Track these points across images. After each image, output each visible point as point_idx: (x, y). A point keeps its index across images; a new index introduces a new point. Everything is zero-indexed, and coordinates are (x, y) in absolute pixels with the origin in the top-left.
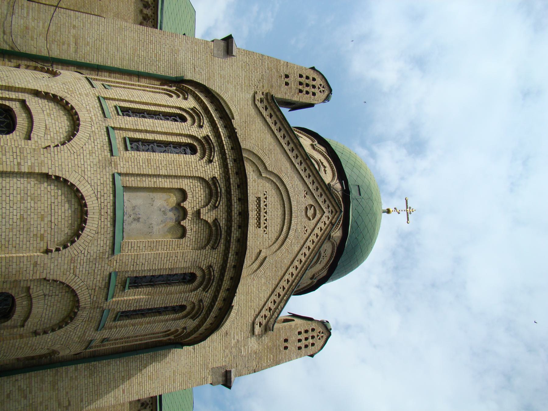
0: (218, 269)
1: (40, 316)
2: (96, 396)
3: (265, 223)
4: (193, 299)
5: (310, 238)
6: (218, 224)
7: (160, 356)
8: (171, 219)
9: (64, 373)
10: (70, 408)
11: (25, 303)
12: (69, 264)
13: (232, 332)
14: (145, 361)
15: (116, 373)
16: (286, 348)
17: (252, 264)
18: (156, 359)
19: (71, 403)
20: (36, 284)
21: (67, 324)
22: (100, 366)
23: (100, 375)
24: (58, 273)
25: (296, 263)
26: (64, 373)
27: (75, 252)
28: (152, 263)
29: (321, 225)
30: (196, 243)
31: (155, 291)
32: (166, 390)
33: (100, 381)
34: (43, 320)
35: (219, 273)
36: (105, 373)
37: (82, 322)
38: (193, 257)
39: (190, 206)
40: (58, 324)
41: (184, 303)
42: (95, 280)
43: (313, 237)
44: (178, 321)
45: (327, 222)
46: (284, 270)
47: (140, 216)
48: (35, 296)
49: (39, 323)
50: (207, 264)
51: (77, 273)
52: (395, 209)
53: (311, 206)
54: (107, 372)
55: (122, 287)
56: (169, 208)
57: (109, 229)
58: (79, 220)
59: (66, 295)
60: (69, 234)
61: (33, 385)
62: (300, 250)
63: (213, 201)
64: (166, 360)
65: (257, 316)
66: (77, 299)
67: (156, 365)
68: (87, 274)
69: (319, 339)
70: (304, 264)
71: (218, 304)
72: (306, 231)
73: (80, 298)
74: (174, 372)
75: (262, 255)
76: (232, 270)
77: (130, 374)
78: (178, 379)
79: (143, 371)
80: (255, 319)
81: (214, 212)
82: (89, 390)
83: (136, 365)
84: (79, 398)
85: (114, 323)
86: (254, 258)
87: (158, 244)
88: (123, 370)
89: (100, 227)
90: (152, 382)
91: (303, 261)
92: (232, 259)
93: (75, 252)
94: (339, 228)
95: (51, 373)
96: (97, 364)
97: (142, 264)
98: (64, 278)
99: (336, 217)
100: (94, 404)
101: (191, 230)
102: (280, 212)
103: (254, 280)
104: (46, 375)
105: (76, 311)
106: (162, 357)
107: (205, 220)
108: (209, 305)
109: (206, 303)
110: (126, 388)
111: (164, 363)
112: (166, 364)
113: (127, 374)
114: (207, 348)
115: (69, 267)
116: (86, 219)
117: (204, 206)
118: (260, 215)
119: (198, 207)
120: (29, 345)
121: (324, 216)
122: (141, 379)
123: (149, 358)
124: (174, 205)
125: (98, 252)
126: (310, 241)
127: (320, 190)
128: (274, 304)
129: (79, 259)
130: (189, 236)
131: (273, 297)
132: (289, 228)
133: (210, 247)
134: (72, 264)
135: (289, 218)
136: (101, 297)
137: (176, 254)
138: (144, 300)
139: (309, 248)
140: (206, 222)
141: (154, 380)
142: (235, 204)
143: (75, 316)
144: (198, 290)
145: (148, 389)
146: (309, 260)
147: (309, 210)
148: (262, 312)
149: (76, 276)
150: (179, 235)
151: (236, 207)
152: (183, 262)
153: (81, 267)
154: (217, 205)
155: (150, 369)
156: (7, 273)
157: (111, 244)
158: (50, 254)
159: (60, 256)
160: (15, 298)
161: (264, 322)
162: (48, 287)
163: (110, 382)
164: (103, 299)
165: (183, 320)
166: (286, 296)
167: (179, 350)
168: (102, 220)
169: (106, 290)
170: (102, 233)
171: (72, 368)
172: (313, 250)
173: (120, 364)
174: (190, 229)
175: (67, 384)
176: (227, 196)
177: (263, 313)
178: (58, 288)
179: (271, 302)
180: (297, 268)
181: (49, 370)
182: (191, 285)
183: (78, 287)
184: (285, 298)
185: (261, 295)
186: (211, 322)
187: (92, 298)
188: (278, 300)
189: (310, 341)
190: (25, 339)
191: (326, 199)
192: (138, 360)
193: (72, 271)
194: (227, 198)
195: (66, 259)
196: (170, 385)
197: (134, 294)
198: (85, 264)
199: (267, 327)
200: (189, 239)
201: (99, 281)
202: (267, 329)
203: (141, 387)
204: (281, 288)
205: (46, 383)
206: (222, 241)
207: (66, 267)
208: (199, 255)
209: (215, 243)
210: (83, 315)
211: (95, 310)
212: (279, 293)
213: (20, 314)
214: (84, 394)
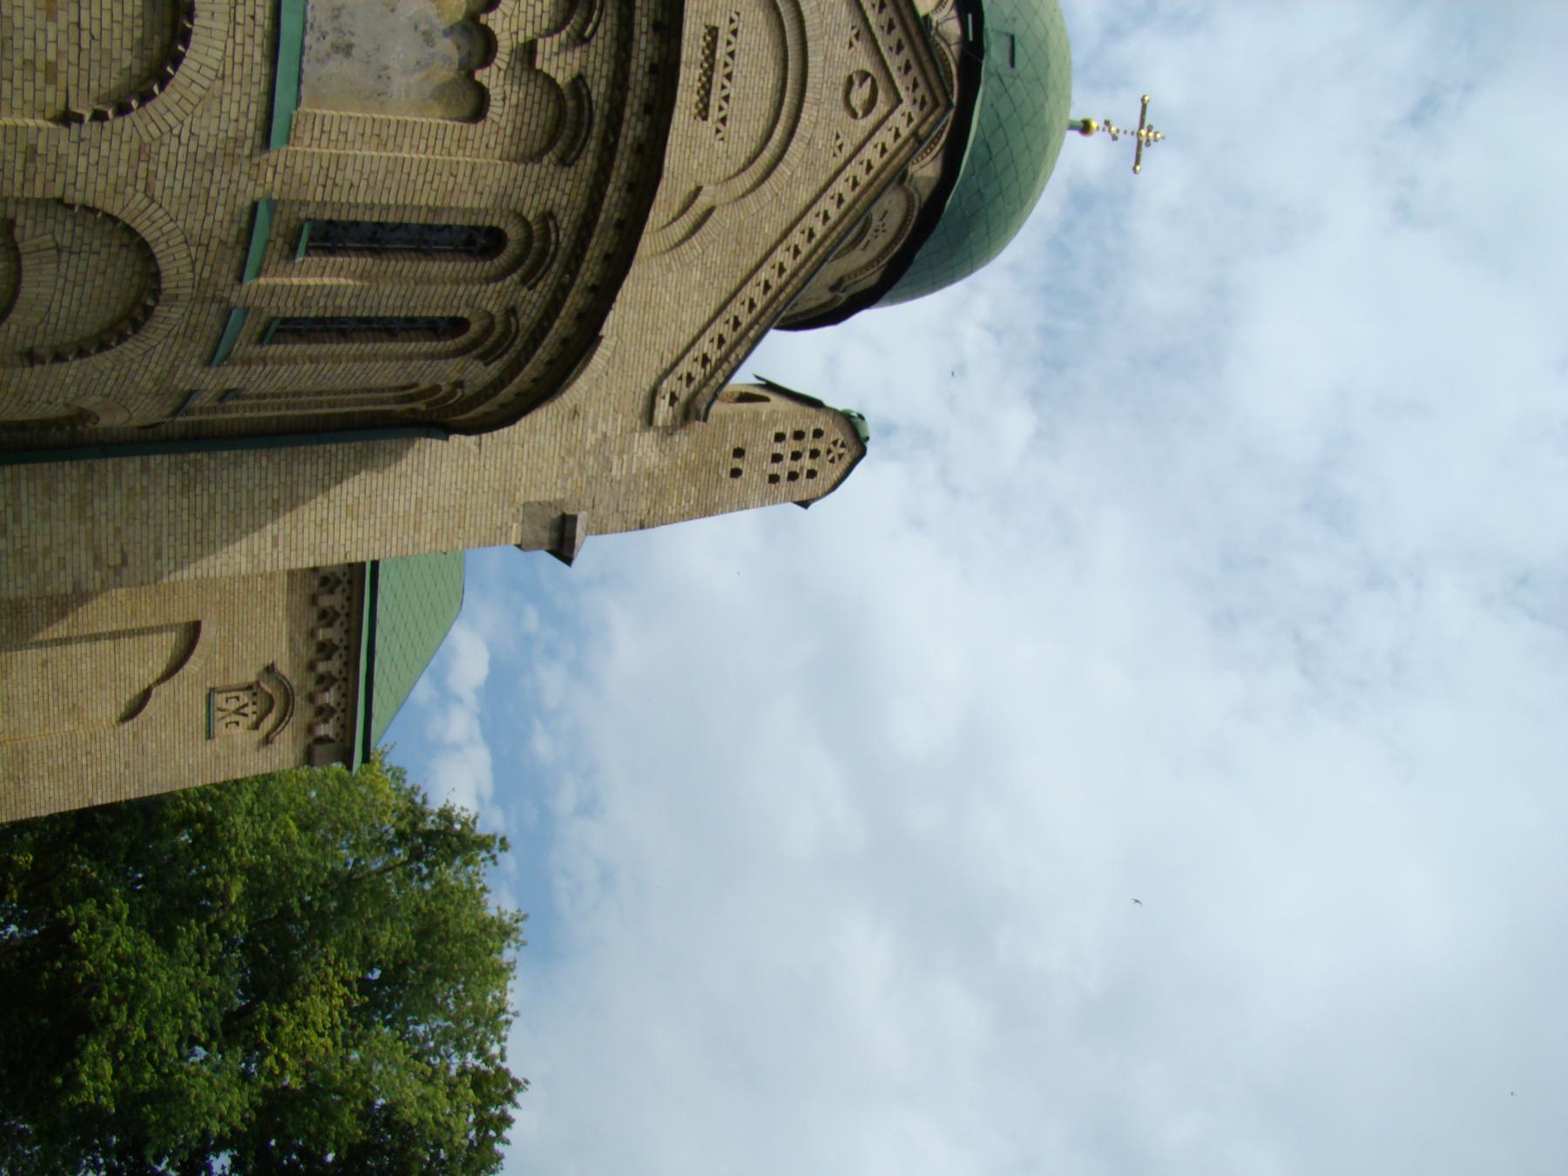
0: (570, 227)
1: (44, 310)
3: (721, 109)
4: (491, 303)
5: (849, 171)
6: (584, 92)
7: (382, 454)
8: (446, 58)
9: (110, 475)
10: (125, 571)
14: (340, 464)
16: (736, 473)
17: (670, 223)
18: (370, 462)
19: (130, 559)
20: (32, 212)
21: (122, 338)
22: (212, 466)
23: (212, 490)
24: (100, 187)
25: (797, 238)
26: (110, 475)
27: (152, 128)
28: (379, 185)
29: (885, 136)
30: (515, 140)
31: (383, 268)
33: (212, 508)
34: (53, 320)
35: (573, 238)
37: (168, 336)
38: (503, 183)
39: (506, 26)
41: (464, 313)
42: (209, 219)
43: (856, 170)
44: (442, 363)
45: (905, 132)
46: (760, 253)
47: (353, 40)
48: (29, 249)
49: (41, 328)
50: (541, 208)
51: (158, 193)
52: (1107, 123)
53: (865, 75)
54: (231, 484)
55: (286, 247)
56: (442, 24)
57: (257, 70)
58: (167, 32)
60: (136, 71)
61: (24, 499)
62: (814, 202)
63: (576, 19)
64: (398, 468)
65: (667, 373)
66: (153, 270)
69: (832, 461)
71: (561, 326)
72: (840, 147)
74: (419, 501)
75: (703, 201)
76: (611, 233)
77: (294, 497)
78: (429, 523)
79: (332, 491)
81: (577, 54)
82: (179, 530)
83: (314, 473)
85: (258, 349)
87: (401, 130)
88: (276, 483)
89: (229, 61)
91: (818, 235)
92: (615, 199)
93: (152, 128)
94: (934, 153)
95: (75, 472)
96: (206, 460)
97: (352, 186)
98: (119, 204)
99: (931, 119)
100: (193, 566)
101: (504, 99)
102: (770, 82)
103: (669, 269)
104: (60, 478)
105: (150, 303)
106: (388, 457)
107: (547, 77)
108: (533, 326)
109: (526, 320)
110: (281, 533)
111: (392, 475)
114: (517, 447)
116: (189, 32)
117: (549, 33)
118: (710, 80)
119: (529, 34)
120: (12, 389)
121: (897, 113)
122: (325, 512)
124: (460, 17)
125: (222, 135)
126: (847, 180)
127: (898, 32)
128: (719, 347)
129: (164, 151)
130: (497, 118)
131: (720, 327)
132: (790, 134)
133: (554, 158)
134: (143, 165)
135: (795, 102)
136: (224, 271)
137: (454, 165)
138: (349, 291)
139: (841, 200)
140: (550, 81)
141: (361, 519)
142: (644, 38)
143: (146, 319)
144: (508, 281)
145: (342, 542)
146: (834, 235)
147: (857, 83)
148: (681, 364)
149: (152, 200)
150: (467, 111)
151: (643, 45)
152: (470, 195)
154: (587, 33)
155: (354, 488)
157: (261, 116)
158: (75, 126)
159: (106, 134)
161: (684, 393)
162: (69, 226)
163: (237, 512)
164: (231, 276)
165: (458, 359)
166: (756, 327)
167: (436, 444)
168: (239, 40)
169: (239, 253)
170: (237, 78)
171: (133, 464)
172: (850, 207)
173: (270, 465)
174: (499, 97)
175: (118, 505)
176: (620, 9)
177: (685, 367)
179: (712, 341)
180: (797, 252)
181: (67, 463)
182: (488, 263)
183: (158, 234)
184: (752, 334)
185: (686, 317)
186: (535, 375)
187: (198, 269)
188: (730, 337)
189: (806, 462)
191: (912, 63)
192: (321, 461)
193: (141, 186)
194: (620, 16)
195: (125, 147)
197: (319, 272)
198: (181, 168)
199: (692, 409)
200: (495, 128)
201: (220, 221)
202: (690, 413)
203: (325, 534)
204: (743, 303)
205: (61, 500)
206: (592, 144)
207: (123, 170)
208: (520, 178)
209: (570, 147)
210: (170, 316)
212: (736, 318)
214: (164, 539)
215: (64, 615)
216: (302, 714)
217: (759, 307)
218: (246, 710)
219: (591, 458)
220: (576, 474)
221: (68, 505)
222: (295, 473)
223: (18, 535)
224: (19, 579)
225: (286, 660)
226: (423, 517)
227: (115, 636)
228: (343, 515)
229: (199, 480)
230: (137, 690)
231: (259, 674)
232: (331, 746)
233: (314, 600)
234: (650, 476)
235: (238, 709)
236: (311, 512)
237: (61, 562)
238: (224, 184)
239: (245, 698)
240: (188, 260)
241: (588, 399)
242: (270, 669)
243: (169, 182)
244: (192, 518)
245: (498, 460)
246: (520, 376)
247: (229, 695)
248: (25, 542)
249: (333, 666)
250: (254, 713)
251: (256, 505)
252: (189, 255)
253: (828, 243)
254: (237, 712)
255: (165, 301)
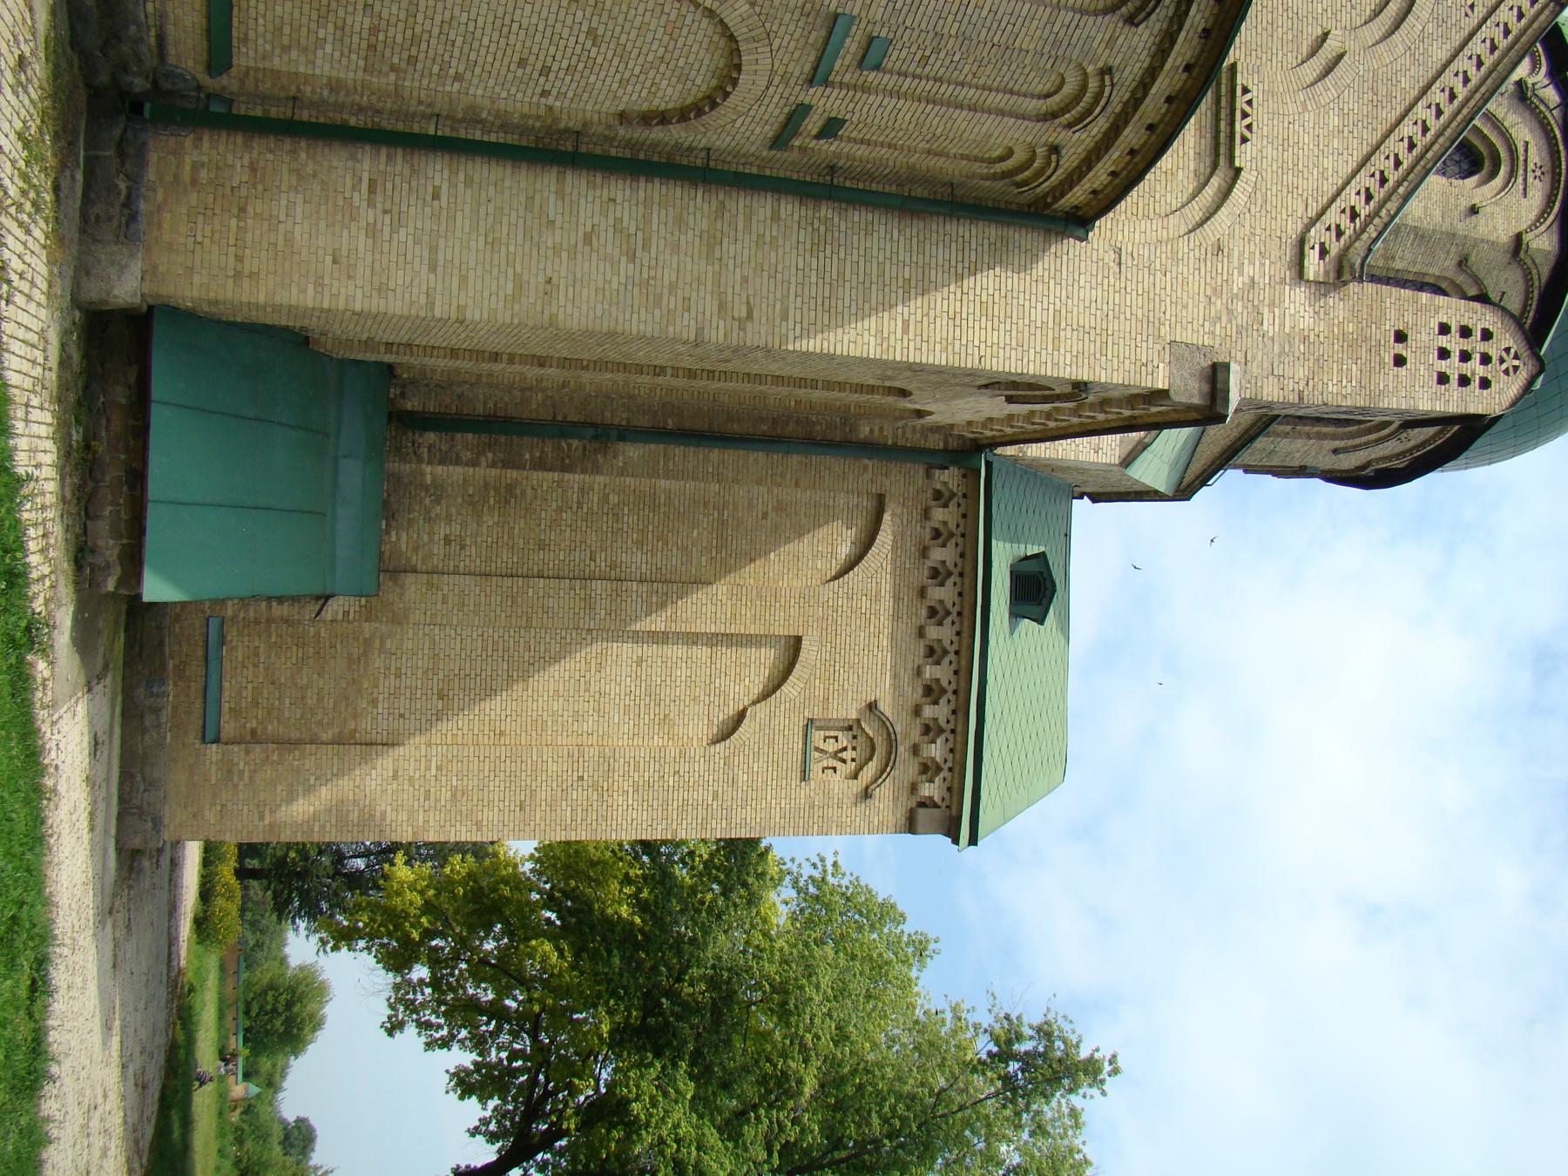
2: (826, 315)
7: (1016, 251)
9: (741, 217)
10: (749, 325)
13: (1236, 249)
14: (973, 253)
15: (888, 262)
16: (1400, 361)
18: (1004, 257)
22: (843, 228)
23: (842, 255)
26: (741, 217)
32: (1031, 364)
33: (841, 274)
36: (855, 251)
44: (1092, 19)
46: (1399, 110)
54: (862, 253)
61: (655, 227)
64: (1034, 271)
65: (1313, 222)
67: (1003, 274)
69: (1506, 372)
70: (1463, 105)
77: (926, 279)
78: (1069, 342)
79: (965, 282)
80: (1307, 229)
82: (806, 289)
83: (947, 257)
84: (778, 305)
86: (1305, 51)
88: (908, 260)
90: (989, 324)
91: (1460, 97)
95: (706, 206)
96: (836, 220)
100: (819, 336)
103: (1305, 109)
104: (691, 210)
106: (1023, 255)
110: (913, 317)
112: (1034, 284)
113: (920, 278)
122: (958, 303)
123: (986, 247)
126: (1484, 41)
131: (1364, 180)
141: (996, 319)
145: (977, 343)
146: (1478, 96)
148: (1328, 212)
155: (988, 282)
161: (1335, 248)
163: (867, 285)
166: (1406, 184)
167: (1072, 246)
171: (763, 206)
173: (902, 238)
175: (746, 252)
177: (1332, 217)
179: (1358, 193)
180: (1439, 113)
184: (1401, 190)
185: (1328, 163)
188: (1379, 194)
189: (1475, 368)
196: (1044, 352)
199: (1345, 263)
203: (958, 329)
204: (1387, 158)
205: (690, 233)
212: (1382, 172)
214: (792, 298)
215: (662, 606)
216: (906, 769)
217: (1405, 165)
218: (844, 755)
219: (1240, 304)
220: (1224, 319)
221: (697, 240)
222: (927, 254)
223: (646, 263)
224: (643, 311)
225: (889, 699)
226: (1062, 333)
227: (715, 640)
228: (978, 311)
229: (829, 241)
230: (731, 711)
231: (860, 711)
232: (936, 811)
233: (921, 632)
234: (1305, 339)
235: (836, 753)
236: (944, 301)
237: (686, 302)
239: (844, 740)
241: (1231, 236)
242: (872, 707)
244: (820, 281)
245: (1140, 285)
246: (1173, 55)
247: (827, 734)
248: (652, 273)
249: (939, 712)
250: (853, 760)
251: (887, 282)
253: (1472, 103)
254: (835, 755)
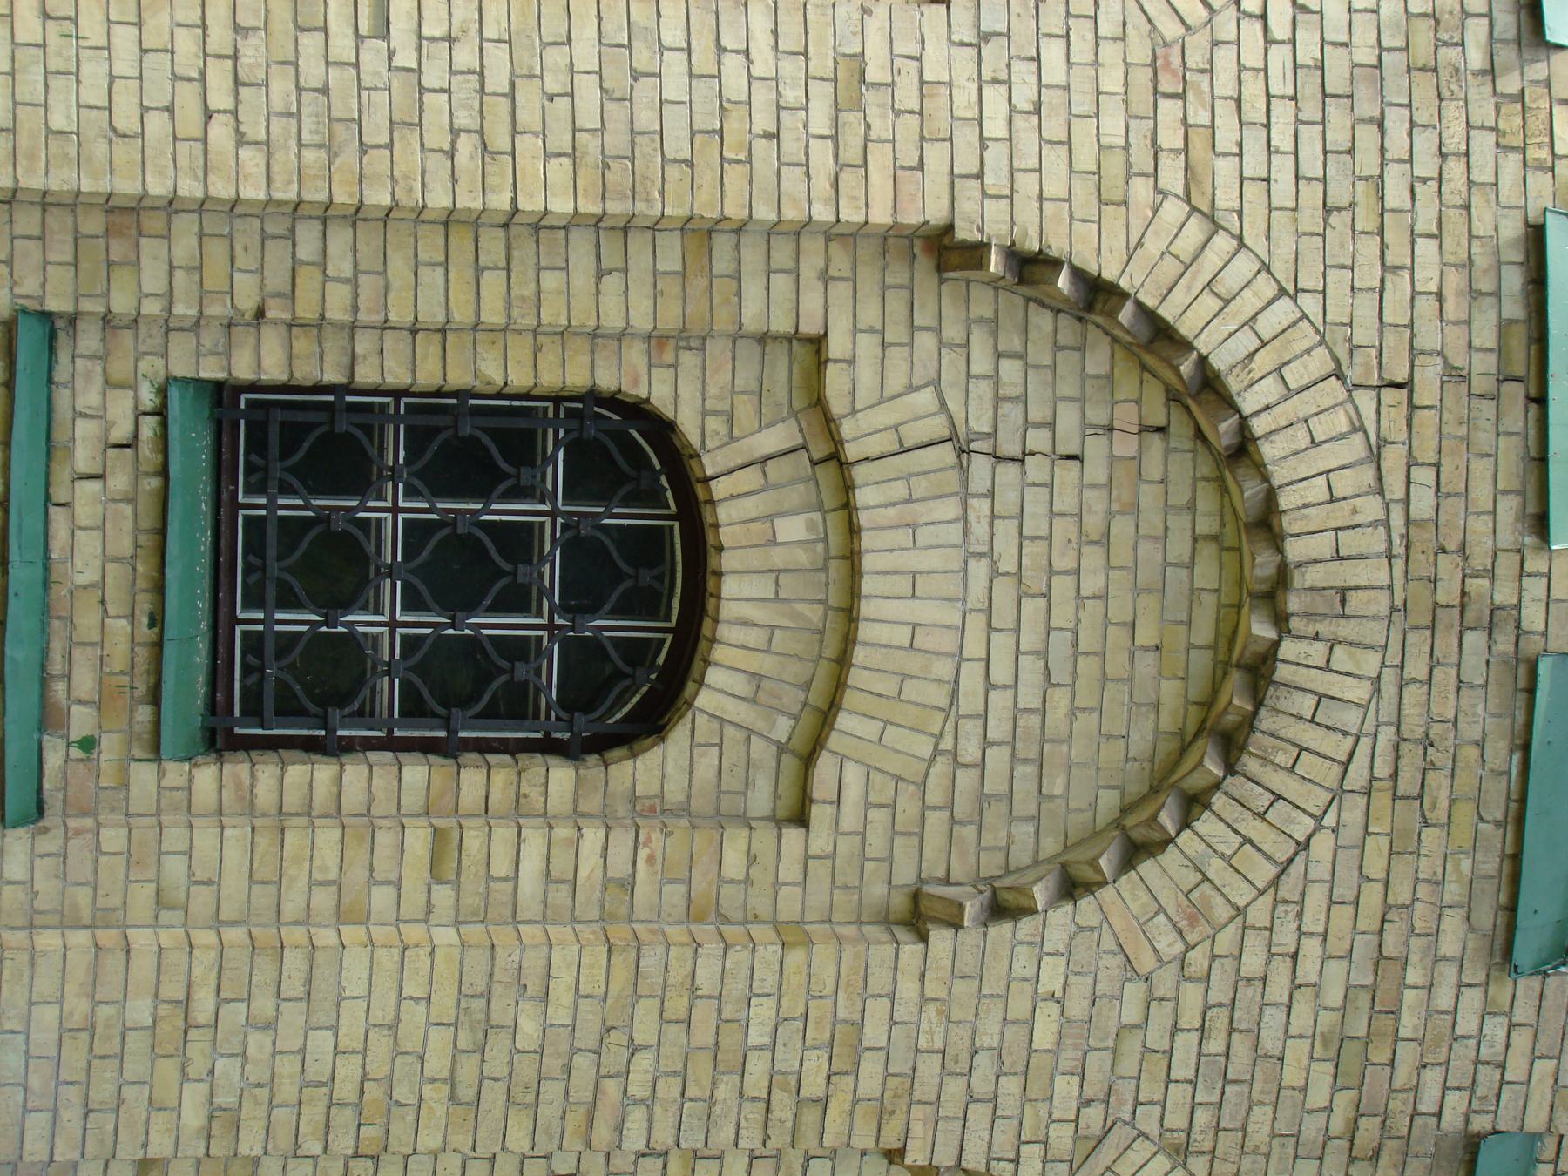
1: (941, 697)
11: (793, 529)
12: (1141, 98)
20: (869, 314)
21: (1194, 804)
34: (970, 751)
37: (1338, 793)
40: (1117, 824)
42: (1399, 288)
48: (874, 446)
49: (935, 796)
51: (1226, 198)
59: (1153, 468)
66: (1252, 489)
68: (1311, 218)
73: (1279, 475)
98: (1115, 243)
115: (1141, 129)
120: (871, 1068)
129: (1225, 60)
136: (1482, 493)
149: (1211, 218)
153: (1254, 141)
156: (617, 141)
160: (710, 464)
162: (981, 364)
164: (1508, 507)
169: (1516, 415)
178: (1068, 387)
183: (1247, 341)
187: (1395, 488)
190: (823, 954)
193: (1172, 177)
195: (1109, 52)
198: (1283, 114)
207: (1113, 126)
211: (1446, 643)
213: (763, 664)
238: (1426, 165)
240: (1355, 447)
243: (1254, 164)
252: (1358, 428)
255: (1307, 615)
